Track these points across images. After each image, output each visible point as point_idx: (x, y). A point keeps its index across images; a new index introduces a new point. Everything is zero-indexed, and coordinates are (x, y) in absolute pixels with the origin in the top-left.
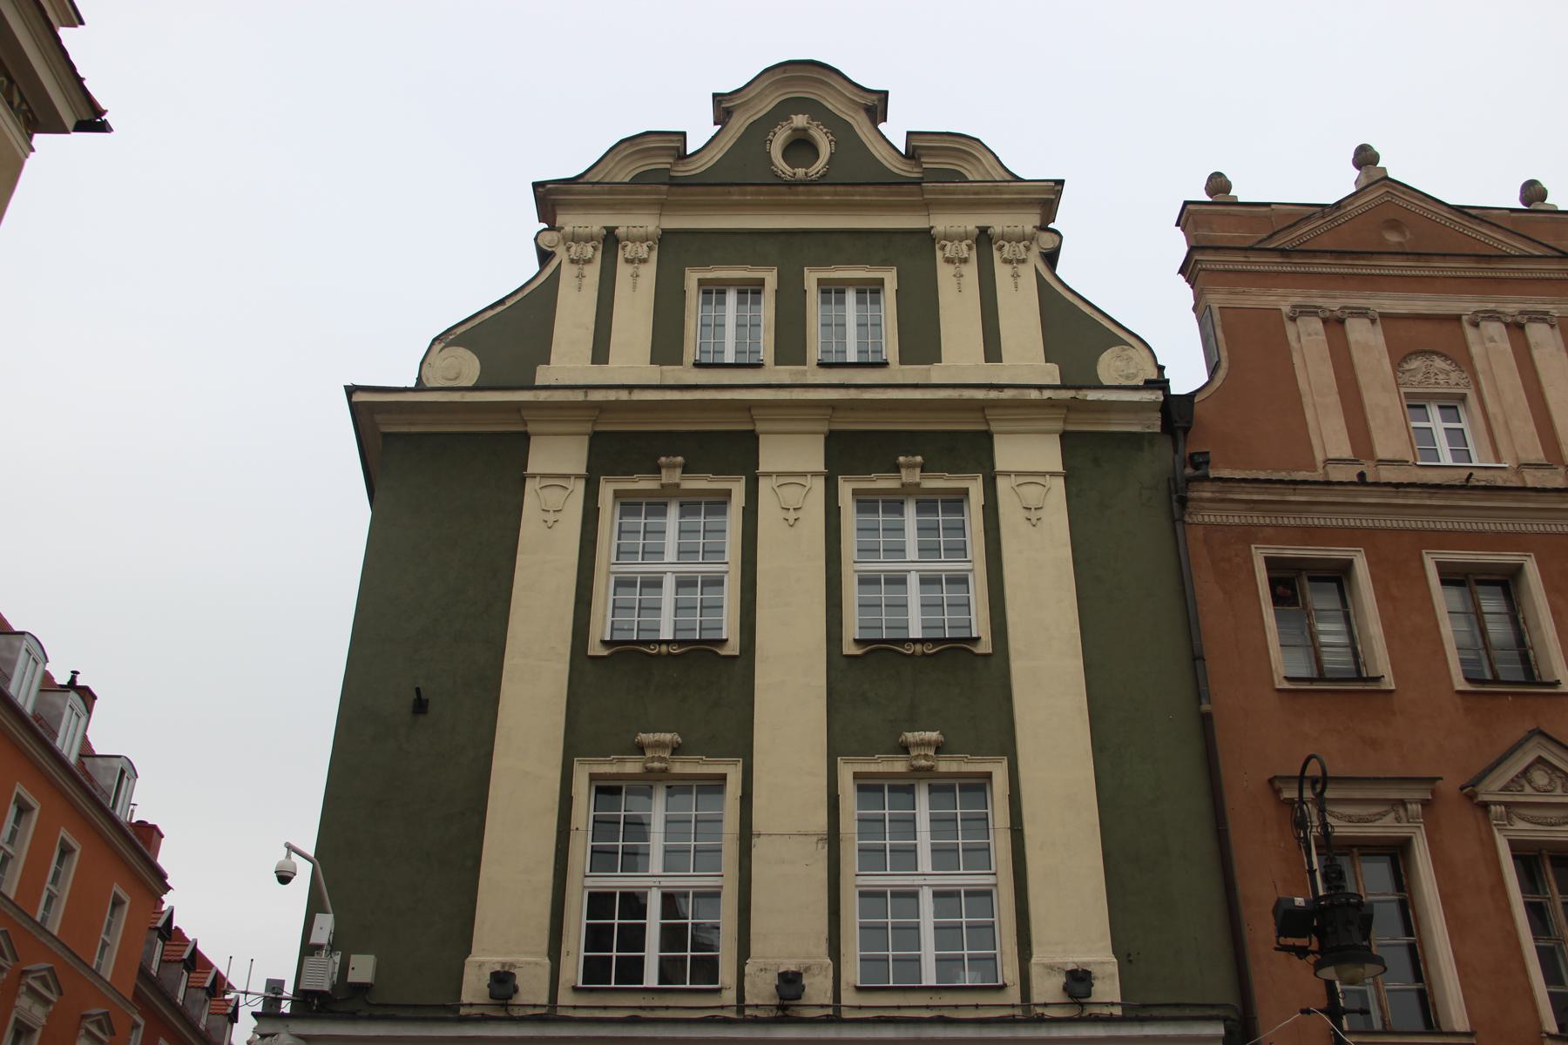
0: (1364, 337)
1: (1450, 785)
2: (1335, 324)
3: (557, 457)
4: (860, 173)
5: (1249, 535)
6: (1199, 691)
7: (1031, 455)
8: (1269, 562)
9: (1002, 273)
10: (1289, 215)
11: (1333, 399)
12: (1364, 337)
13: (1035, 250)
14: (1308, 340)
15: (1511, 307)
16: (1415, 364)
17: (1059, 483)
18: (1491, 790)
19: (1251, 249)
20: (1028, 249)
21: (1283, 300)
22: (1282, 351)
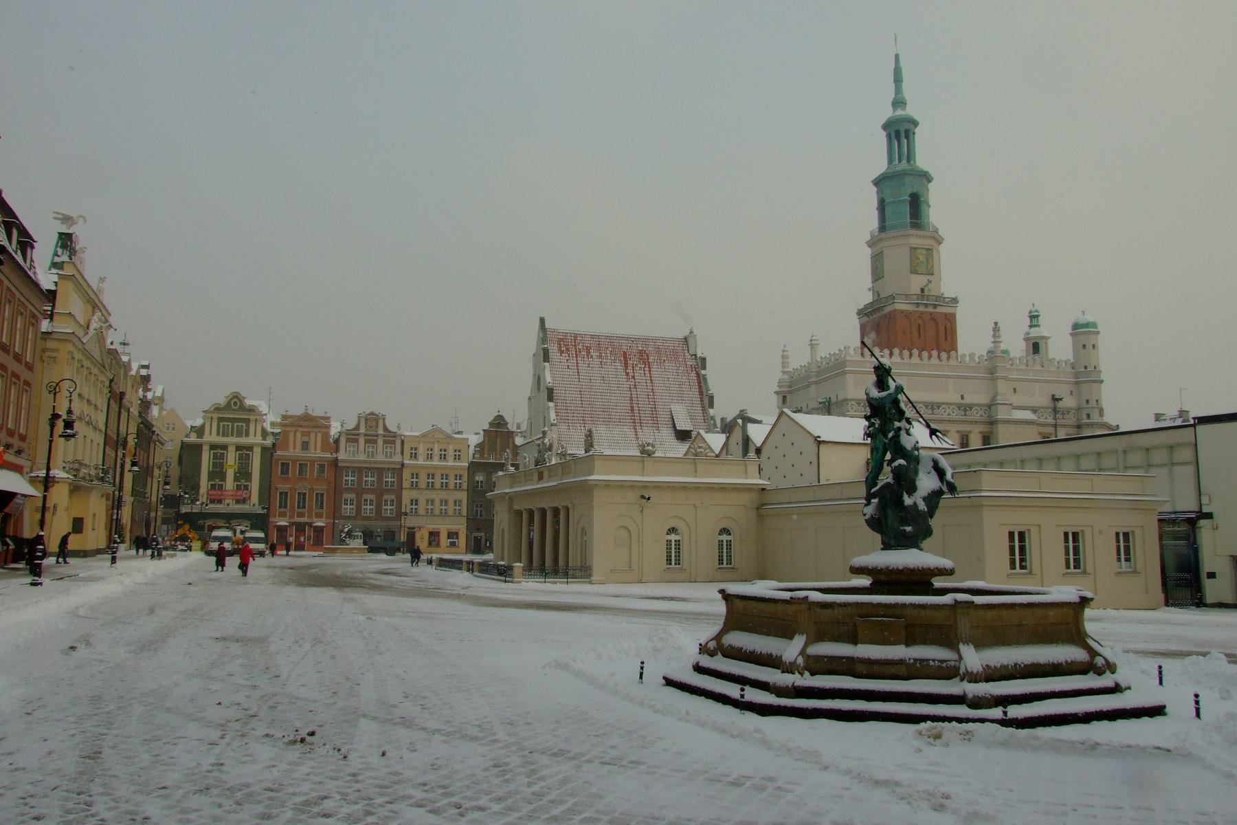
0: (299, 435)
3: (206, 448)
4: (242, 408)
7: (257, 450)
12: (299, 435)
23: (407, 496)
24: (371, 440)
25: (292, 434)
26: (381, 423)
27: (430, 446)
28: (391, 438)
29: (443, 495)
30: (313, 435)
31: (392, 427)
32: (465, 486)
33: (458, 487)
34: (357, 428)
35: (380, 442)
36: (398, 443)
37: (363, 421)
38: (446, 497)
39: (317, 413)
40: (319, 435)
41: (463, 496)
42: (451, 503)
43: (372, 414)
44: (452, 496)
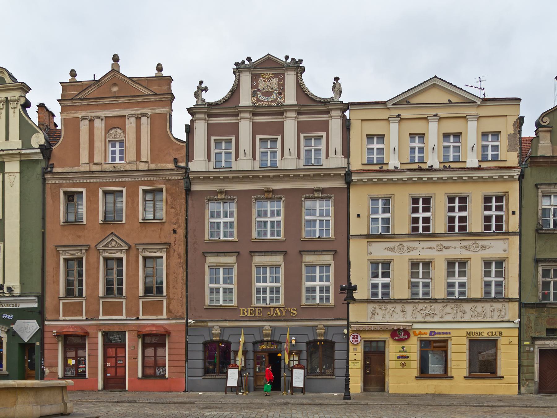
0: (99, 125)
1: (93, 245)
2: (91, 121)
5: (60, 186)
6: (44, 227)
8: (65, 193)
9: (11, 111)
10: (87, 84)
11: (87, 146)
12: (99, 125)
13: (20, 103)
14: (84, 126)
15: (139, 112)
16: (113, 131)
17: (18, 175)
18: (100, 247)
19: (72, 99)
20: (17, 104)
21: (79, 114)
22: (77, 131)
23: (360, 255)
24: (268, 128)
25: (84, 126)
26: (290, 78)
27: (417, 127)
28: (315, 110)
29: (456, 250)
30: (131, 124)
31: (320, 89)
32: (513, 224)
33: (495, 229)
34: (235, 91)
35: (290, 126)
36: (336, 125)
37: (246, 79)
38: (463, 254)
39: (136, 67)
40: (145, 122)
41: (507, 249)
42: (476, 269)
43: (269, 62)
44: (476, 254)
